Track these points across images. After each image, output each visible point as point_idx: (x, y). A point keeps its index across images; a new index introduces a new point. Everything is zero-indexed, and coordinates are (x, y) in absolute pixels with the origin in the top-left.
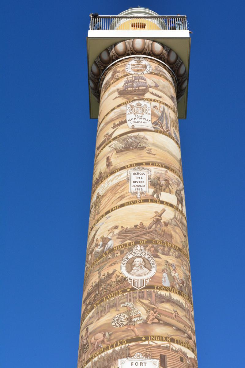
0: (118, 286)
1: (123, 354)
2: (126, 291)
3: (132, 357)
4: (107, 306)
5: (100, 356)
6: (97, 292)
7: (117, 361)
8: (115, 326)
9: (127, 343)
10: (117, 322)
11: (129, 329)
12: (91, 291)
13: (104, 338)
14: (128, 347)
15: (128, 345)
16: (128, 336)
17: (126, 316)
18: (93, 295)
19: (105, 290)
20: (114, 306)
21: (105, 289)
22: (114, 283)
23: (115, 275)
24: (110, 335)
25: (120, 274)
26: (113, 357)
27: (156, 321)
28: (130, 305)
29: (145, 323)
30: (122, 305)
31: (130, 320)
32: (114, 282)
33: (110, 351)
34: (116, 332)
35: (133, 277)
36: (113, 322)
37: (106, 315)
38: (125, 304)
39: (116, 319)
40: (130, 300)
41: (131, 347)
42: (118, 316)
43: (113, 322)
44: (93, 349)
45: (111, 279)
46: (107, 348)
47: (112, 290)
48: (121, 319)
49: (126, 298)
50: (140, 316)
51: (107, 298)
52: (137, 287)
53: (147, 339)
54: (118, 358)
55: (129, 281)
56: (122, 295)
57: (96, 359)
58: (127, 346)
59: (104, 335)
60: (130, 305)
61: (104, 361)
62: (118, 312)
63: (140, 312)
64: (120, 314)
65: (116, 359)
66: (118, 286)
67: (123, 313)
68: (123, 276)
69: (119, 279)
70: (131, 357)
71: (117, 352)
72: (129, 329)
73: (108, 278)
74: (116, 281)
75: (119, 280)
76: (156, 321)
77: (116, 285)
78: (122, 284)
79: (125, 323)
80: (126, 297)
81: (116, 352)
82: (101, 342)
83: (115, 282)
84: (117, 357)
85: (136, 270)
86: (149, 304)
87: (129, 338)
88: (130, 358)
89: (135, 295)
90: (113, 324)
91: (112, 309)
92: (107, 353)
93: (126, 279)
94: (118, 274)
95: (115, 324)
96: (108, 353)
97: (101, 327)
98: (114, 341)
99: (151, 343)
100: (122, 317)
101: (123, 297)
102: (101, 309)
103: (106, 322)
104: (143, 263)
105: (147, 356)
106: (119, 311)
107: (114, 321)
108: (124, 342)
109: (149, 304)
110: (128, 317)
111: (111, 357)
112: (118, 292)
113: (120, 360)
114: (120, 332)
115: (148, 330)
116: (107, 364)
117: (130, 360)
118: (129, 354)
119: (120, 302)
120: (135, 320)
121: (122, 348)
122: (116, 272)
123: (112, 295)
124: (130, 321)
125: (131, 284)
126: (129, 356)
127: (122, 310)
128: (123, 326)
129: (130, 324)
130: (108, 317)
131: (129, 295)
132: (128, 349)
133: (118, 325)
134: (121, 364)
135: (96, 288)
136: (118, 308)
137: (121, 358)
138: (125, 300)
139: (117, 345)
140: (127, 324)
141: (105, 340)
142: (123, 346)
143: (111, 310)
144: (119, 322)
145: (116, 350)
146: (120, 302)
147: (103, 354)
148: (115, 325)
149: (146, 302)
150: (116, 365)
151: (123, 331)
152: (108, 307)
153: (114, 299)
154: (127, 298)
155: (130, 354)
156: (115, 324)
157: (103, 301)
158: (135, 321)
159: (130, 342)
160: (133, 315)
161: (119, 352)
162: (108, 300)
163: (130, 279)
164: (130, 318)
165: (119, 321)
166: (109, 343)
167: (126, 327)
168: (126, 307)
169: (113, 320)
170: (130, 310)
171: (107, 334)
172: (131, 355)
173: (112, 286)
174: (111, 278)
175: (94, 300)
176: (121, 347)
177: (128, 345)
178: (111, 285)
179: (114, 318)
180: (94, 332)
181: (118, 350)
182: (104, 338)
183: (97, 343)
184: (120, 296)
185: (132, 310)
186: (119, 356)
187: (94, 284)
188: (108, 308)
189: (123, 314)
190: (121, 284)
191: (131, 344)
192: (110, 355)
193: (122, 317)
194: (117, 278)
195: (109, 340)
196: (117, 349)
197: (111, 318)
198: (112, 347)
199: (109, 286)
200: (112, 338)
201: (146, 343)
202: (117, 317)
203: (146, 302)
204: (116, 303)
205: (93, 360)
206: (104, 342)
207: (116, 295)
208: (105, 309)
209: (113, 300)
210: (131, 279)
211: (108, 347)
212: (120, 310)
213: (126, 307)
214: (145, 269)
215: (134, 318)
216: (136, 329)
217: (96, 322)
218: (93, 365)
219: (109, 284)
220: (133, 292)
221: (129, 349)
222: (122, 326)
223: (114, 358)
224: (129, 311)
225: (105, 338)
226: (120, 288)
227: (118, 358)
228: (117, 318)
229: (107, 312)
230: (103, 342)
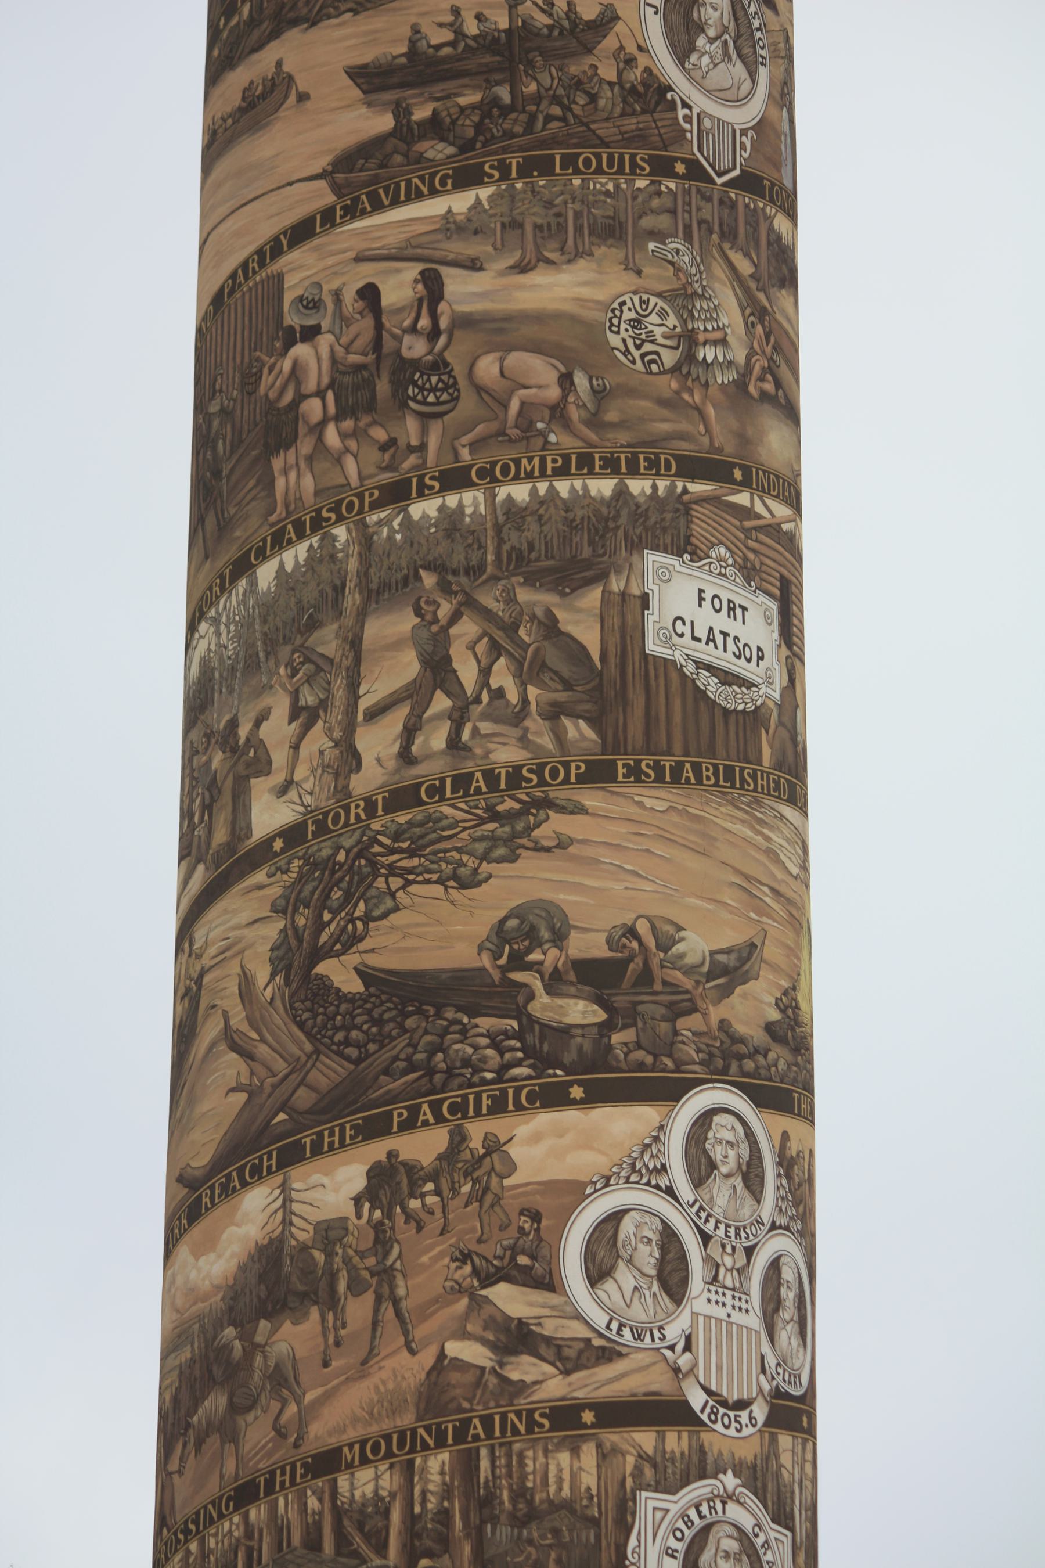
0: (631, 124)
1: (664, 530)
2: (662, 168)
3: (701, 559)
4: (577, 215)
5: (542, 487)
6: (504, 93)
7: (635, 558)
8: (624, 354)
9: (679, 474)
10: (631, 333)
11: (686, 396)
12: (448, 59)
13: (564, 397)
14: (686, 498)
15: (685, 491)
16: (682, 437)
17: (672, 320)
18: (470, 98)
19: (557, 111)
20: (612, 231)
21: (556, 100)
22: (606, 87)
23: (610, 43)
24: (600, 394)
25: (640, 48)
26: (618, 528)
27: (769, 387)
28: (686, 259)
29: (741, 384)
30: (652, 246)
31: (690, 348)
32: (611, 84)
33: (603, 487)
34: (631, 392)
35: (700, 102)
36: (612, 325)
37: (571, 267)
38: (665, 244)
39: (628, 315)
40: (688, 237)
41: (696, 502)
42: (636, 299)
43: (612, 325)
44: (494, 426)
45: (591, 60)
46: (586, 465)
47: (604, 130)
48: (651, 328)
49: (668, 211)
50: (723, 342)
51: (569, 161)
52: (713, 168)
53: (746, 483)
54: (640, 538)
55: (681, 112)
56: (652, 188)
57: (520, 492)
58: (679, 490)
59: (566, 380)
60: (686, 259)
61: (570, 523)
62: (630, 280)
63: (724, 320)
64: (645, 297)
65: (636, 546)
66: (631, 124)
67: (659, 295)
68: (655, 71)
69: (635, 75)
70: (695, 558)
71: (638, 506)
72: (686, 396)
73: (574, 44)
74: (620, 82)
75: (633, 86)
76: (769, 387)
77: (618, 110)
78: (647, 117)
79: (669, 358)
80: (669, 204)
81: (634, 508)
82: (547, 413)
83: (616, 89)
84: (638, 531)
85: (705, 60)
86: (753, 285)
87: (684, 447)
88: (692, 560)
89: (706, 213)
90: (615, 340)
91: (603, 249)
92: (585, 487)
93: (669, 96)
94: (631, 48)
95: (624, 341)
96: (593, 493)
97: (539, 318)
98: (623, 437)
99: (759, 508)
100: (654, 318)
101: (655, 203)
102: (534, 216)
103: (568, 307)
104: (732, 26)
105: (749, 573)
106: (639, 273)
107: (615, 321)
108: (668, 467)
109: (753, 285)
110: (678, 330)
111: (607, 520)
112: (633, 157)
113: (652, 558)
114: (646, 397)
115: (750, 432)
116: (586, 552)
117: (689, 572)
118: (688, 542)
119: (647, 222)
120: (709, 360)
121: (660, 493)
122: (619, 27)
123: (598, 157)
124: (690, 357)
125: (689, 135)
126: (689, 548)
127: (658, 277)
128: (660, 373)
129: (689, 373)
130: (586, 284)
131: (684, 202)
132: (684, 506)
133: (636, 354)
134: (657, 581)
135: (488, 59)
136: (637, 256)
137: (656, 548)
138: (663, 222)
139: (633, 471)
140: (676, 369)
141: (574, 413)
142: (662, 485)
143: (600, 251)
144: (643, 341)
145: (631, 495)
146: (647, 222)
147: (563, 487)
148: (623, 349)
149: (745, 267)
150: (633, 577)
151: (662, 402)
152: (582, 226)
153: (610, 187)
154: (673, 212)
155: (694, 540)
156: (624, 341)
157: (545, 167)
158: (708, 365)
159: (693, 477)
160: (702, 328)
161: (647, 510)
162: (577, 182)
163: (685, 105)
164: (688, 340)
165: (643, 336)
166: (593, 436)
167: (674, 385)
168: (672, 263)
169: (610, 314)
170: (689, 291)
171: (580, 380)
172: (696, 547)
173: (602, 103)
174: (589, 51)
175: (479, 128)
176: (655, 487)
177: (685, 491)
178: (593, 98)
179: (616, 305)
180: (499, 330)
181: (642, 500)
182: (564, 397)
183: (523, 404)
184: (641, 183)
185: (695, 293)
186: (646, 529)
187: (472, 28)
188: (579, 230)
189: (661, 303)
190: (644, 112)
191: (696, 488)
192: (604, 510)
193: (654, 318)
194: (621, 65)
195: (595, 422)
196: (638, 486)
197: (601, 295)
198: (611, 466)
199: (582, 99)
200: (612, 416)
201: (742, 498)
202: (629, 304)
203: (745, 267)
204: (623, 219)
205: (502, 492)
206: (562, 416)
207: (621, 171)
208: (562, 228)
209: (607, 193)
210: (690, 108)
211: (591, 456)
212: (647, 270)
213: (671, 268)
214: (739, 70)
215: (705, 344)
216: (711, 411)
217: (501, 274)
218: (501, 519)
219: (578, 84)
220: (698, 191)
221: (687, 511)
222: (654, 367)
223: (620, 533)
224: (683, 297)
225: (571, 399)
226: (638, 139)
227: (640, 538)
228: (633, 315)
229: (578, 255)
230: (557, 412)
